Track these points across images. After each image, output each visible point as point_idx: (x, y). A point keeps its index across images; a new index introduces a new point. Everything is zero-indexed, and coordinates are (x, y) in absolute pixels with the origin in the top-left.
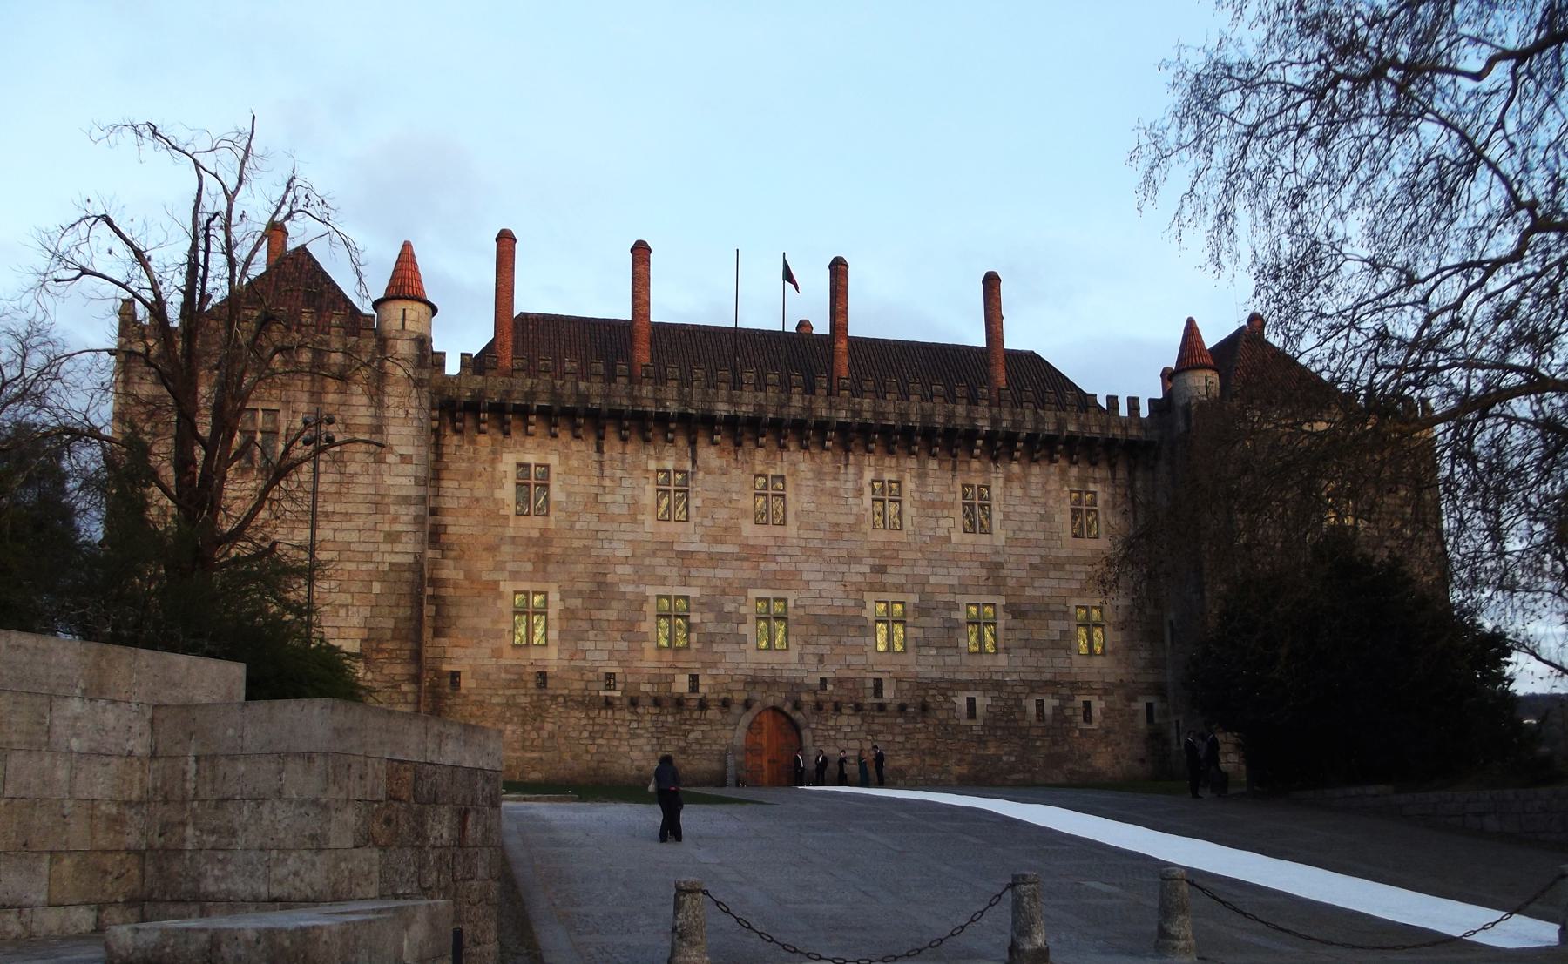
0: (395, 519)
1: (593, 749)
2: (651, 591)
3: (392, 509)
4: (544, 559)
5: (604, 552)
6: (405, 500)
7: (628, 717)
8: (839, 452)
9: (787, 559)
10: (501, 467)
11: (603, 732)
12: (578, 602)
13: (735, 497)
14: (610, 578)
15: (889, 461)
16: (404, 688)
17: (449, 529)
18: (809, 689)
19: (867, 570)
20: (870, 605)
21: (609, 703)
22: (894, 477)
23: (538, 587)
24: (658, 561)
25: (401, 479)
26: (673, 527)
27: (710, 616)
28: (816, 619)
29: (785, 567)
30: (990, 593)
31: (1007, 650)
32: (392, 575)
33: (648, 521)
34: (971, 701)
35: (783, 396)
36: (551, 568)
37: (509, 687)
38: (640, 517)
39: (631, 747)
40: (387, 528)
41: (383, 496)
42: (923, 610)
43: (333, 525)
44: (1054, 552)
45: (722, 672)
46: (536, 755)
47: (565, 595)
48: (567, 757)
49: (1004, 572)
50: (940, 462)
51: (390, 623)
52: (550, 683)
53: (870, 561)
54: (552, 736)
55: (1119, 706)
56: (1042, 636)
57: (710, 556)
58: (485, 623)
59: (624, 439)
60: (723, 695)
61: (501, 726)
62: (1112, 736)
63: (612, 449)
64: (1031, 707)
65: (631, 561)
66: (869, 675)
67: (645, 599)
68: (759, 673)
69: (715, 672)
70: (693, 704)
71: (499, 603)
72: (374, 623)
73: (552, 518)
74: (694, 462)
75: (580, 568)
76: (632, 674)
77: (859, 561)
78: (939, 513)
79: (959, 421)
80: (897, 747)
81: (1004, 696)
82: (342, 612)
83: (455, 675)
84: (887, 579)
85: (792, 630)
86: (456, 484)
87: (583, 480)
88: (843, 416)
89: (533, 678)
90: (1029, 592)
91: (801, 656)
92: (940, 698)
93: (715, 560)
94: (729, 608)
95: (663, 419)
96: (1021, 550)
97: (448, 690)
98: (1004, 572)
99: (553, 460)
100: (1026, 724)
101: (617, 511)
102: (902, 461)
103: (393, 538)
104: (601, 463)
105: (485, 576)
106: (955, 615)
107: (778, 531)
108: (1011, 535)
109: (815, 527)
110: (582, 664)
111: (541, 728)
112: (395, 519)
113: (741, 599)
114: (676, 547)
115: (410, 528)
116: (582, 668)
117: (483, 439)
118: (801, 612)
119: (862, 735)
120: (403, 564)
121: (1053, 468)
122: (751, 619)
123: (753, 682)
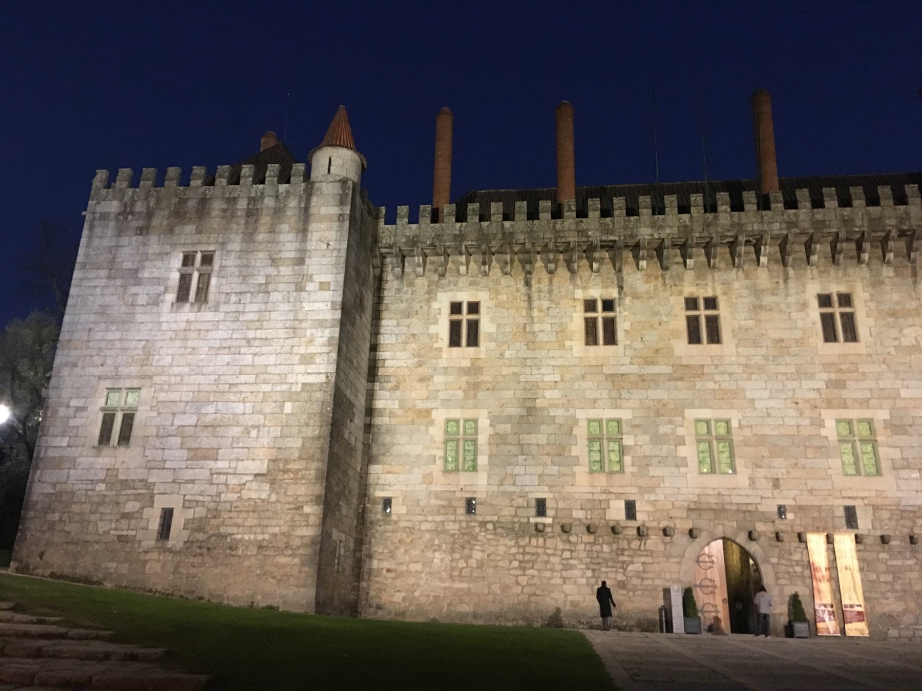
1: (523, 580)
3: (309, 332)
4: (475, 387)
5: (530, 378)
6: (321, 324)
7: (561, 546)
9: (726, 377)
10: (435, 305)
11: (534, 562)
12: (509, 426)
13: (665, 319)
14: (539, 403)
16: (307, 509)
17: (387, 363)
18: (764, 518)
19: (822, 385)
20: (830, 424)
21: (539, 530)
22: (843, 289)
23: (470, 414)
24: (587, 384)
26: (601, 350)
27: (645, 438)
28: (761, 440)
29: (724, 385)
32: (305, 394)
35: (710, 216)
36: (481, 395)
37: (438, 514)
38: (568, 343)
39: (565, 579)
40: (302, 350)
41: (301, 321)
42: (897, 427)
43: (253, 350)
45: (661, 497)
46: (464, 585)
47: (495, 420)
48: (496, 589)
50: (896, 269)
51: (298, 443)
52: (479, 509)
53: (825, 376)
54: (481, 565)
57: (642, 378)
59: (551, 272)
60: (663, 524)
61: (429, 554)
63: (539, 282)
65: (560, 386)
68: (703, 499)
74: (621, 288)
75: (509, 394)
76: (564, 499)
77: (811, 376)
80: (883, 588)
82: (254, 433)
83: (387, 502)
84: (845, 394)
85: (737, 451)
87: (512, 311)
89: (463, 503)
91: (752, 480)
93: (644, 381)
94: (664, 429)
97: (379, 516)
99: (483, 297)
103: (307, 359)
104: (530, 299)
105: (420, 405)
109: (755, 344)
111: (470, 557)
112: (311, 341)
115: (325, 349)
116: (512, 493)
118: (747, 432)
122: (690, 439)
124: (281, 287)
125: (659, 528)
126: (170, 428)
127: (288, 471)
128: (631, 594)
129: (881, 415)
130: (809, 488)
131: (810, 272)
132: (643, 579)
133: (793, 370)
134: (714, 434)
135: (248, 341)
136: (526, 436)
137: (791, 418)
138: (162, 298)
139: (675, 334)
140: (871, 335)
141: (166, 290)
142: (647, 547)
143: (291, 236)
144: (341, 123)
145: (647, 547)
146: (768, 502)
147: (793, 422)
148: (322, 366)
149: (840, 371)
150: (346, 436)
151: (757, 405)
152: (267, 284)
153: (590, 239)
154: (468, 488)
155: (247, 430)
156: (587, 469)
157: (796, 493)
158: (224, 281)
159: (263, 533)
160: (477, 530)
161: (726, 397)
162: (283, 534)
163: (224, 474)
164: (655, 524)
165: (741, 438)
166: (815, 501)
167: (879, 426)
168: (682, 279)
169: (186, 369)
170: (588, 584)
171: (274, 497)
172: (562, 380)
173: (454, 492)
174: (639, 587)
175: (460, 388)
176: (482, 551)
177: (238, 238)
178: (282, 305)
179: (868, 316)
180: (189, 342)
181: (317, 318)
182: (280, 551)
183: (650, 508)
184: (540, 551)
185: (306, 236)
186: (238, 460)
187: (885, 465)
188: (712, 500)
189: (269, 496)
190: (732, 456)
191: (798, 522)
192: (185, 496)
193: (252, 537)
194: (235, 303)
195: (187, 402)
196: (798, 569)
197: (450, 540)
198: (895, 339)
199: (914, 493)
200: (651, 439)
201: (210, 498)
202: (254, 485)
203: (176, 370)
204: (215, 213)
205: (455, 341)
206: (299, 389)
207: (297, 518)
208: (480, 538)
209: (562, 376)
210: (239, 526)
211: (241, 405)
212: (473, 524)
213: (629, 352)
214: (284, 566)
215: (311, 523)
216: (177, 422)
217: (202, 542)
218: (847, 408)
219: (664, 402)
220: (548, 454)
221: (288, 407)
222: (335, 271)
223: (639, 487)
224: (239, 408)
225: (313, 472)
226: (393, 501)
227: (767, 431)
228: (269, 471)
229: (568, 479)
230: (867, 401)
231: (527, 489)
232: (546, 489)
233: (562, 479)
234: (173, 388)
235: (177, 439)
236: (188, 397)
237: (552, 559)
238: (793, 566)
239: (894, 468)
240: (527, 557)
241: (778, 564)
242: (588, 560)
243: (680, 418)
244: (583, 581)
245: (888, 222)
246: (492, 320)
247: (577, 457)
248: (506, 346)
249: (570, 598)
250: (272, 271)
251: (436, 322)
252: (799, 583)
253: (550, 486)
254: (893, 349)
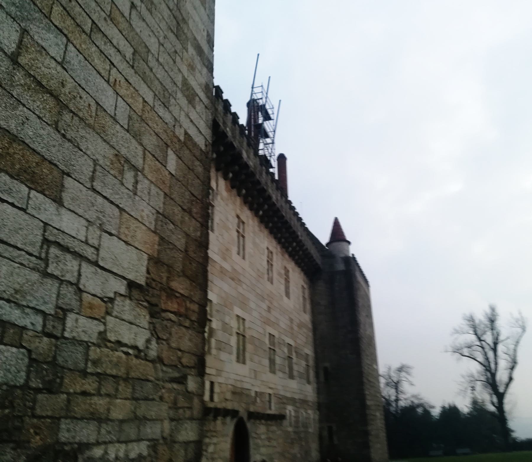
19: (265, 308)
27: (220, 324)
94: (227, 319)
159: (139, 440)
163: (77, 255)
189: (148, 341)
202: (125, 308)
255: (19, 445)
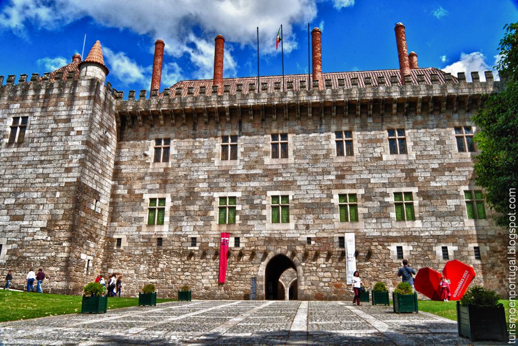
0: (71, 161)
1: (183, 277)
2: (217, 195)
6: (76, 152)
8: (316, 118)
9: (289, 175)
12: (180, 202)
13: (261, 145)
14: (196, 190)
15: (346, 121)
17: (123, 171)
18: (302, 244)
19: (333, 177)
21: (191, 255)
24: (221, 180)
25: (76, 143)
26: (229, 162)
28: (302, 206)
30: (408, 186)
31: (421, 218)
32: (66, 189)
33: (217, 161)
34: (400, 249)
36: (168, 186)
37: (144, 246)
39: (202, 276)
41: (67, 151)
42: (367, 198)
43: (43, 166)
44: (447, 161)
45: (252, 235)
49: (415, 174)
51: (62, 212)
53: (335, 173)
54: (162, 271)
55: (499, 249)
56: (443, 209)
57: (247, 175)
58: (136, 214)
59: (206, 123)
60: (253, 248)
62: (496, 268)
63: (200, 128)
64: (438, 250)
65: (207, 181)
66: (335, 235)
67: (212, 199)
68: (272, 236)
69: (248, 235)
70: (236, 253)
71: (142, 204)
72: (54, 212)
73: (170, 162)
74: (240, 130)
77: (329, 173)
78: (374, 145)
79: (381, 95)
81: (421, 245)
82: (41, 207)
83: (119, 240)
84: (345, 182)
86: (127, 150)
88: (315, 99)
90: (433, 184)
91: (296, 226)
92: (380, 247)
93: (249, 178)
94: (257, 202)
95: (222, 111)
96: (427, 161)
97: (115, 248)
98: (415, 174)
100: (436, 261)
101: (201, 157)
102: (352, 120)
103: (68, 170)
105: (137, 192)
106: (387, 200)
107: (284, 161)
108: (419, 153)
109: (304, 158)
110: (181, 233)
111: (157, 267)
113: (263, 197)
114: (230, 173)
115: (77, 165)
117: (142, 130)
119: (333, 269)
120: (71, 183)
121: (442, 116)
123: (269, 240)
124: (59, 134)
125: (250, 251)
126: (3, 205)
127: (57, 225)
128: (234, 282)
129: (361, 192)
130: (323, 228)
131: (334, 121)
132: (240, 275)
133: (321, 170)
134: (280, 203)
135: (41, 162)
136: (189, 207)
137: (318, 194)
138: (2, 141)
139: (266, 153)
140: (359, 152)
141: (4, 137)
142: (244, 259)
143: (65, 108)
144: (75, 50)
145: (244, 259)
146: (303, 236)
147: (318, 197)
148: (75, 174)
149: (343, 170)
150: (93, 208)
151: (302, 188)
152: (51, 132)
153: (224, 106)
154: (159, 233)
155: (39, 205)
156: (218, 223)
157: (316, 231)
158: (31, 131)
159: (43, 256)
160: (162, 253)
161: (288, 185)
162: (53, 256)
164: (248, 249)
165: (293, 205)
166: (325, 235)
167: (359, 197)
168: (271, 125)
169: (11, 176)
170: (214, 279)
171: (49, 239)
172: (208, 178)
173: (152, 235)
174: (238, 279)
175: (158, 183)
176: (164, 264)
177: (39, 110)
178: (58, 143)
179: (358, 142)
180: (13, 163)
181: (74, 149)
182: (52, 265)
183: (246, 241)
184: (192, 263)
185: (72, 108)
186: (34, 220)
187: (360, 216)
188: (277, 236)
190: (288, 215)
191: (317, 245)
192: (8, 238)
193: (38, 258)
194: (36, 142)
195: (11, 192)
196: (314, 268)
197: (148, 258)
198: (371, 154)
199: (372, 230)
200: (250, 206)
201: (19, 239)
202: (40, 233)
203: (7, 177)
204: (30, 97)
205: (157, 160)
206: (64, 185)
207: (59, 248)
208: (163, 258)
209: (208, 176)
210: (32, 252)
211: (36, 194)
212: (160, 251)
213: (242, 163)
214: (51, 271)
215: (66, 251)
216: (6, 203)
217: (14, 260)
218: (345, 188)
219: (258, 187)
220: (199, 215)
221: (58, 194)
222: (85, 125)
223: (242, 231)
224: (35, 195)
225: (68, 226)
226: (122, 240)
227: (306, 201)
228: (47, 226)
229: (208, 227)
230: (354, 185)
231: (187, 233)
232: (197, 233)
233: (205, 228)
234: (5, 185)
235: (5, 210)
236: (10, 191)
237: (197, 267)
238: (312, 266)
239: (364, 218)
240: (186, 266)
241: (306, 266)
242: (215, 267)
243: (265, 196)
244: (212, 277)
245: (368, 95)
246: (176, 148)
247: (213, 217)
248: (182, 161)
249: (205, 285)
250: (54, 126)
251: (148, 150)
252: (314, 275)
253: (199, 231)
254: (369, 159)
255: (16, 256)
